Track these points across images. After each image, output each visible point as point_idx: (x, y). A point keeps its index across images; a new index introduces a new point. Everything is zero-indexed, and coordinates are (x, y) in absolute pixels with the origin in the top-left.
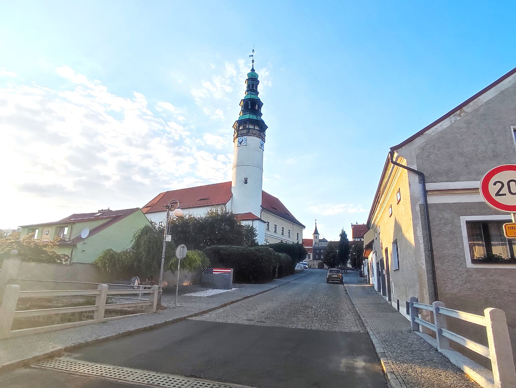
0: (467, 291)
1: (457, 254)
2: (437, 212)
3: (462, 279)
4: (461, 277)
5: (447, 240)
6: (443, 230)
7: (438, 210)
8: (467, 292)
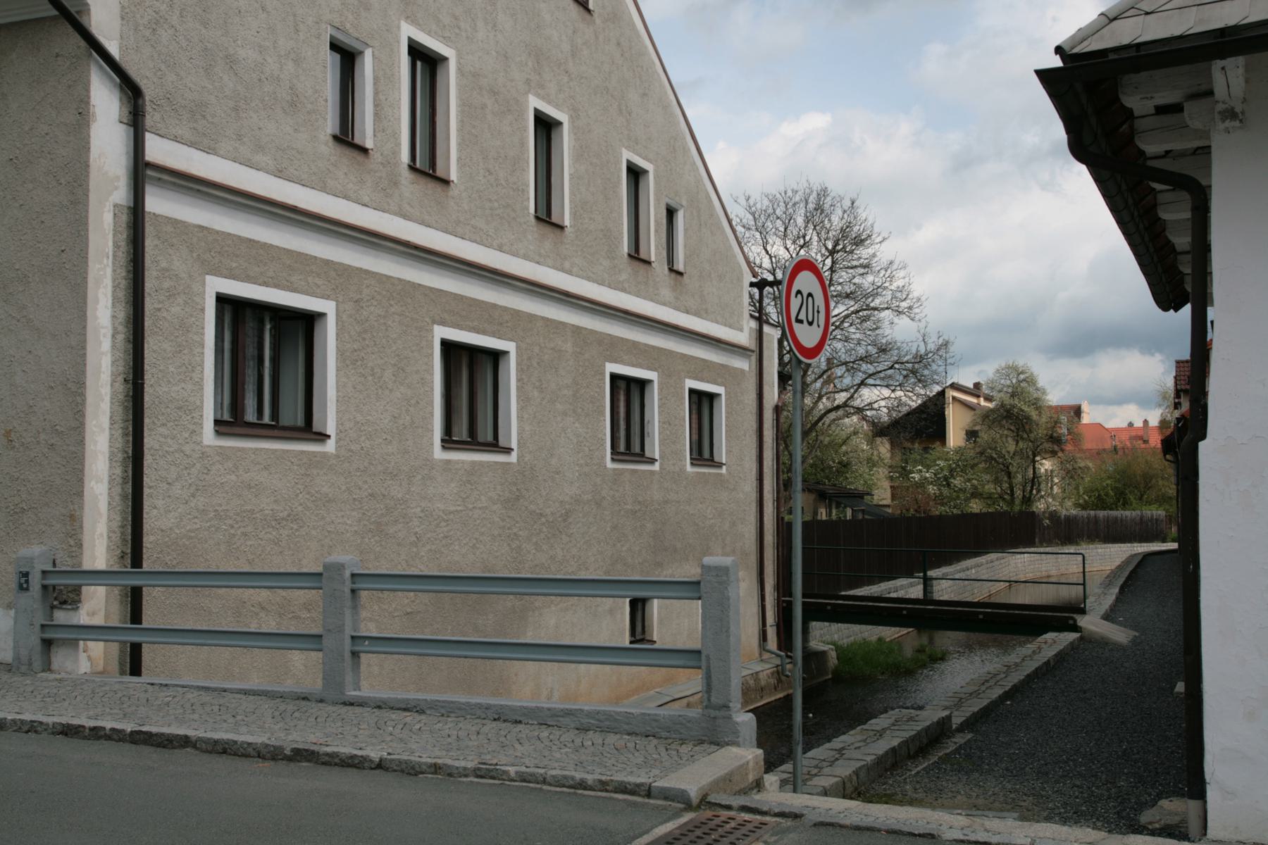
0: (197, 517)
1: (186, 401)
2: (157, 245)
3: (190, 481)
4: (189, 474)
5: (169, 349)
6: (165, 314)
7: (159, 238)
8: (196, 520)
